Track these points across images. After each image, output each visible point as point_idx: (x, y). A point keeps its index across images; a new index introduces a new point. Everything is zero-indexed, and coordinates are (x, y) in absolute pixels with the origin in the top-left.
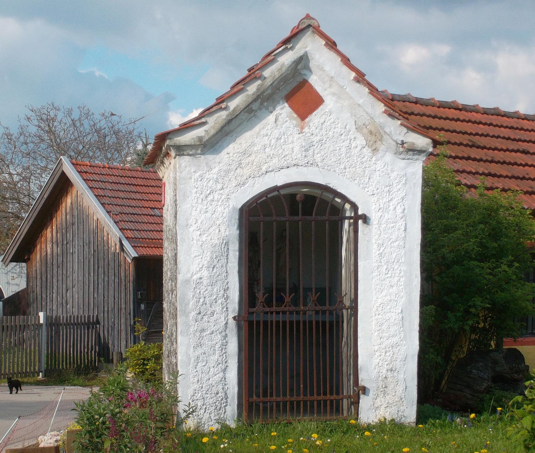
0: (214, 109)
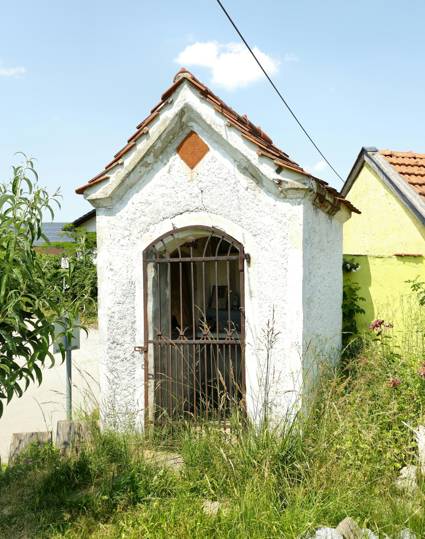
0: (114, 164)
